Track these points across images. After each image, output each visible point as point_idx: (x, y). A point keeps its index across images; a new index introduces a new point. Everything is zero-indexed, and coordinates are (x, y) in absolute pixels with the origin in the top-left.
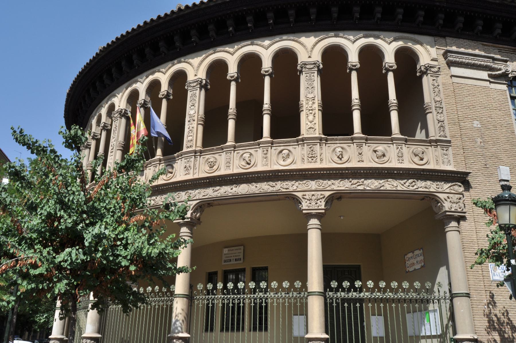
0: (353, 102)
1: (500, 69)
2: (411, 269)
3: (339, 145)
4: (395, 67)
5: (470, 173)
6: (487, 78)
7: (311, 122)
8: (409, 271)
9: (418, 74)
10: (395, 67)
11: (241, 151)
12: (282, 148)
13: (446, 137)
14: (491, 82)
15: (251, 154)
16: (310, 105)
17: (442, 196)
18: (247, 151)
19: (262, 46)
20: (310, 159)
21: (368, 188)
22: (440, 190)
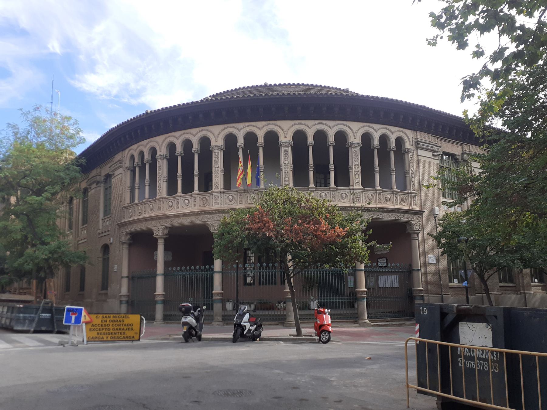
0: (375, 168)
1: (438, 152)
2: (378, 253)
3: (370, 193)
4: (395, 149)
5: (425, 211)
6: (432, 157)
7: (357, 179)
8: (376, 254)
9: (402, 152)
10: (395, 149)
11: (319, 191)
12: (342, 192)
13: (415, 191)
14: (433, 159)
15: (325, 194)
16: (357, 169)
17: (413, 222)
18: (323, 192)
19: (329, 127)
20: (357, 200)
21: (384, 218)
22: (413, 219)
